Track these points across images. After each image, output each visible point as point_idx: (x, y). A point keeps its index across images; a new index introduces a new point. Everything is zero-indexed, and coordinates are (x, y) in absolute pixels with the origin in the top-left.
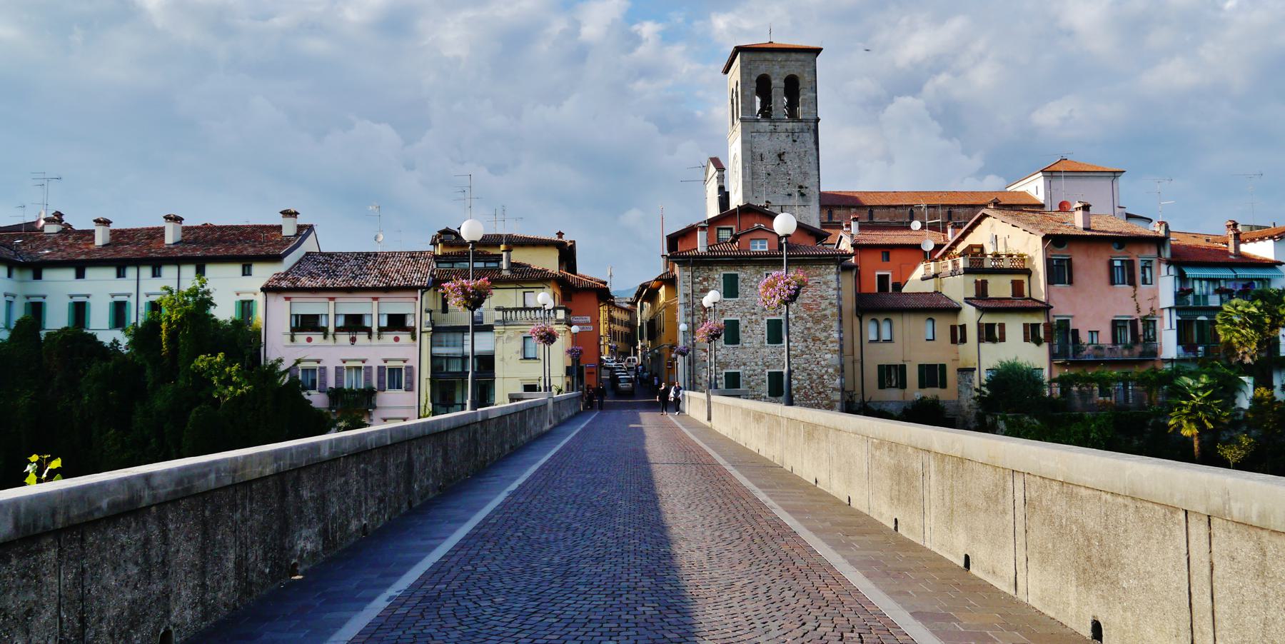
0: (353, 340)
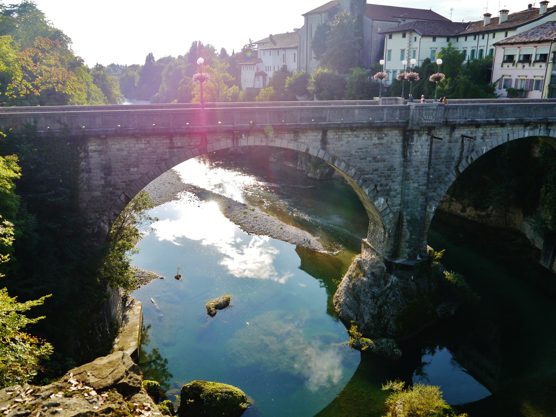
0: (524, 66)
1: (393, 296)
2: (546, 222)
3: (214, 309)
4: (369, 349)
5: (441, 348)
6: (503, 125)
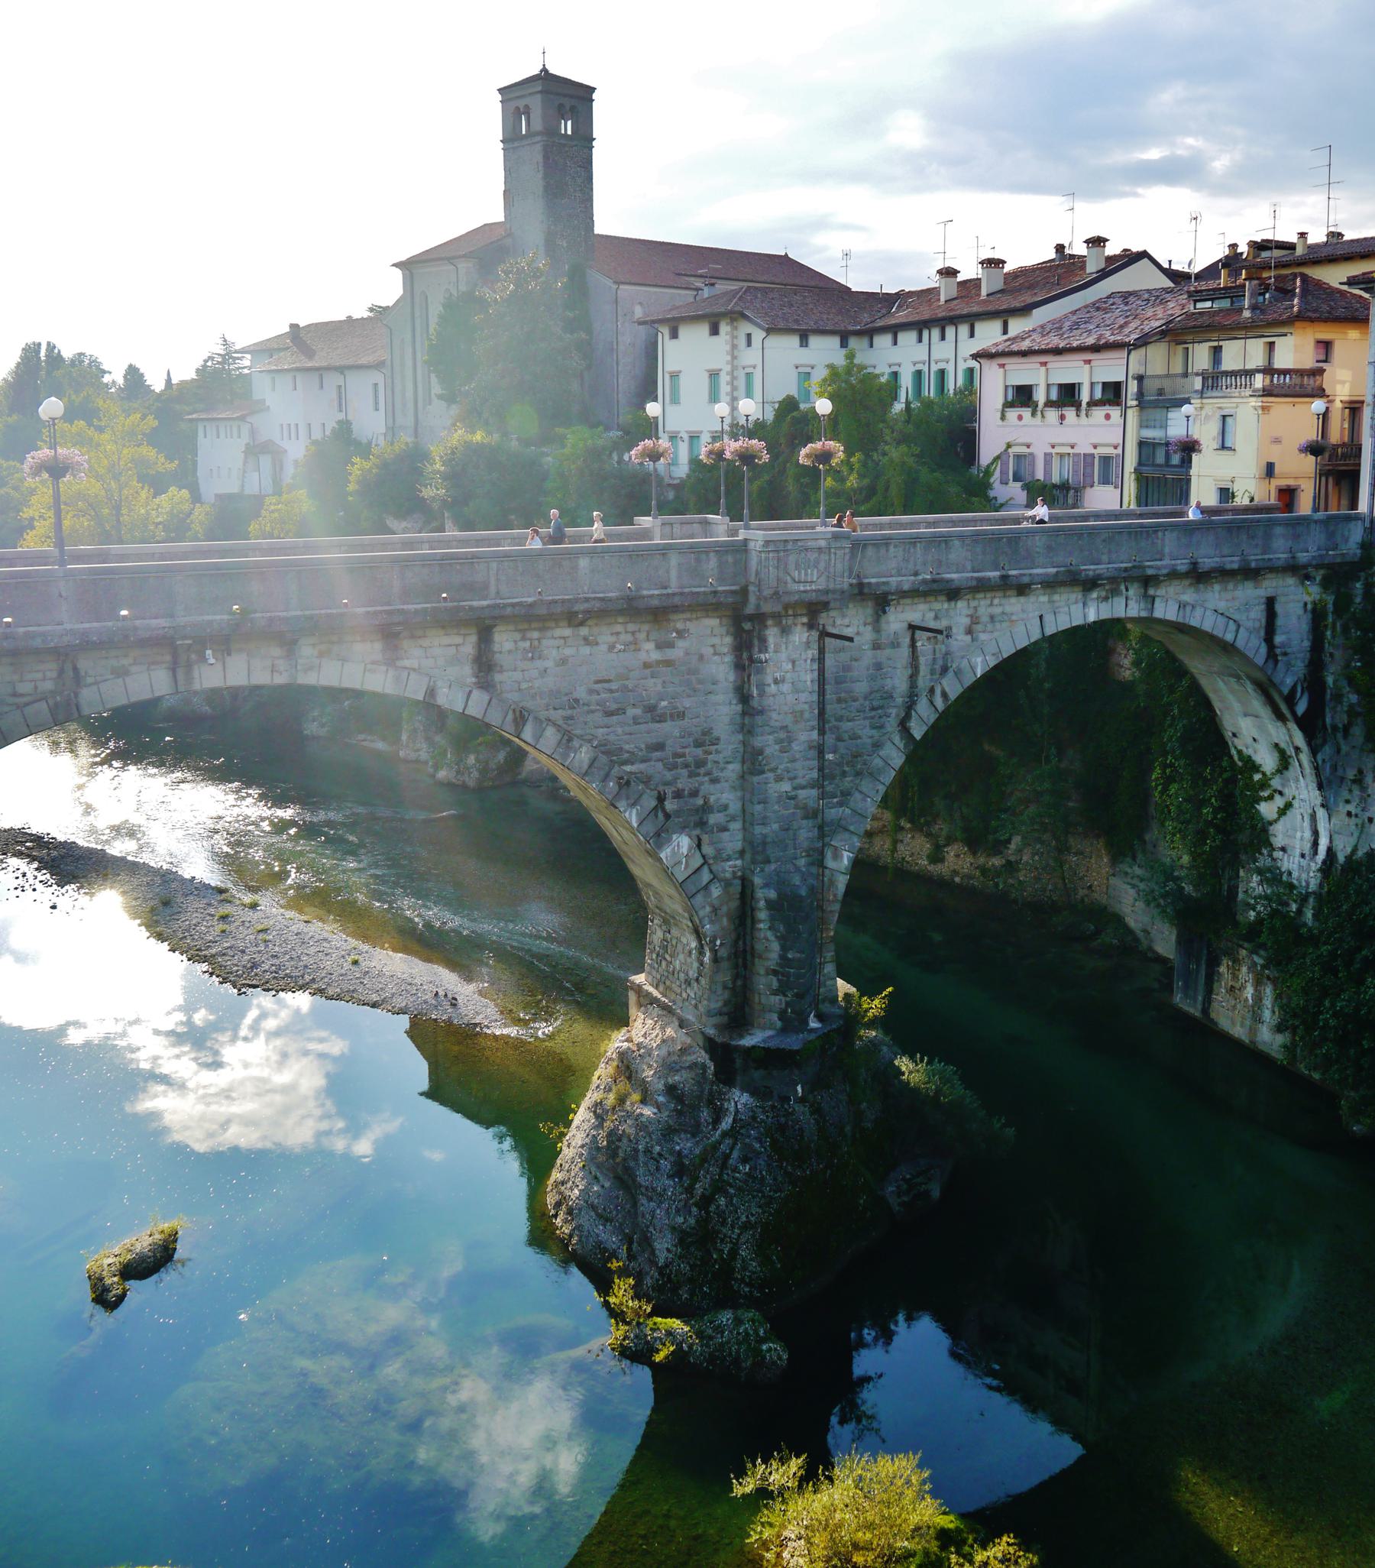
0: (1062, 417)
1: (745, 1160)
2: (1176, 874)
3: (115, 1279)
4: (679, 1356)
5: (909, 1319)
6: (1022, 590)
